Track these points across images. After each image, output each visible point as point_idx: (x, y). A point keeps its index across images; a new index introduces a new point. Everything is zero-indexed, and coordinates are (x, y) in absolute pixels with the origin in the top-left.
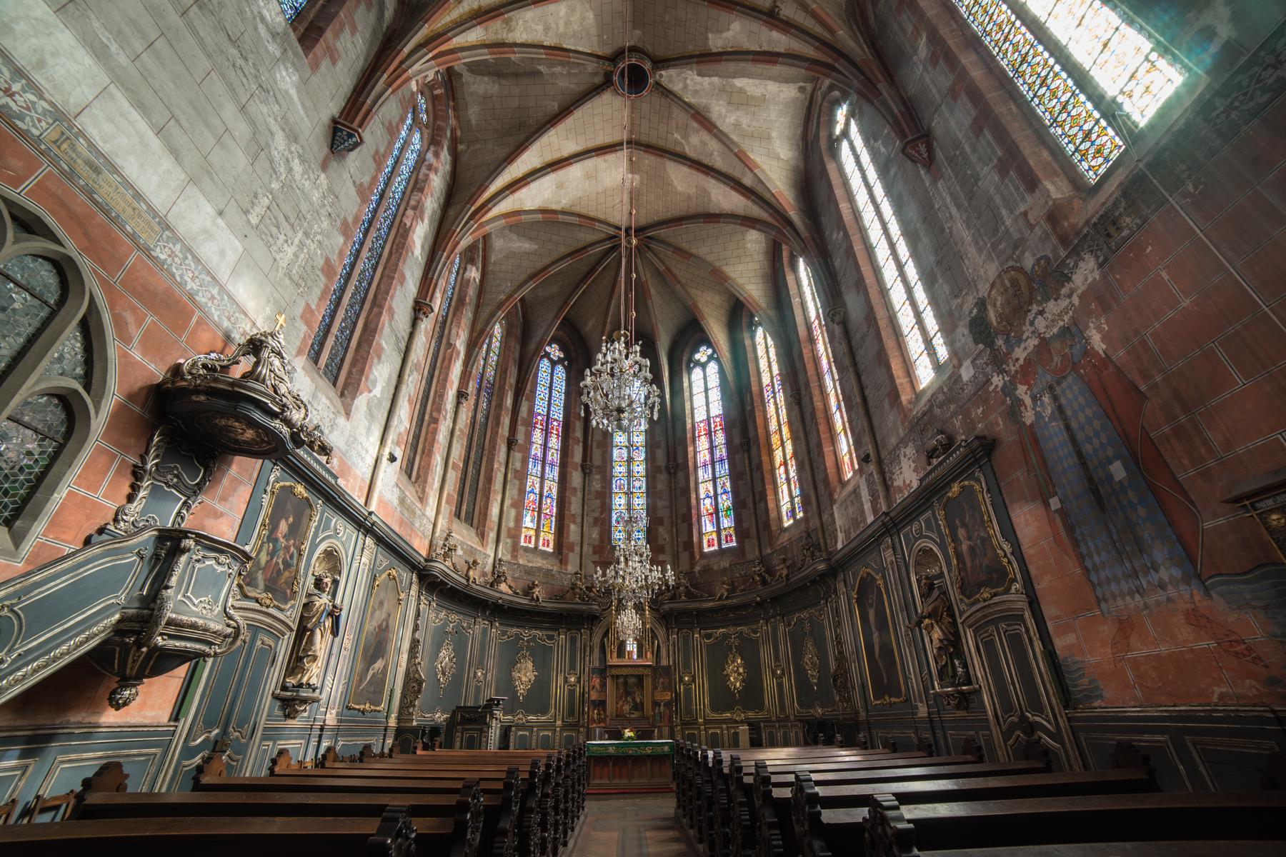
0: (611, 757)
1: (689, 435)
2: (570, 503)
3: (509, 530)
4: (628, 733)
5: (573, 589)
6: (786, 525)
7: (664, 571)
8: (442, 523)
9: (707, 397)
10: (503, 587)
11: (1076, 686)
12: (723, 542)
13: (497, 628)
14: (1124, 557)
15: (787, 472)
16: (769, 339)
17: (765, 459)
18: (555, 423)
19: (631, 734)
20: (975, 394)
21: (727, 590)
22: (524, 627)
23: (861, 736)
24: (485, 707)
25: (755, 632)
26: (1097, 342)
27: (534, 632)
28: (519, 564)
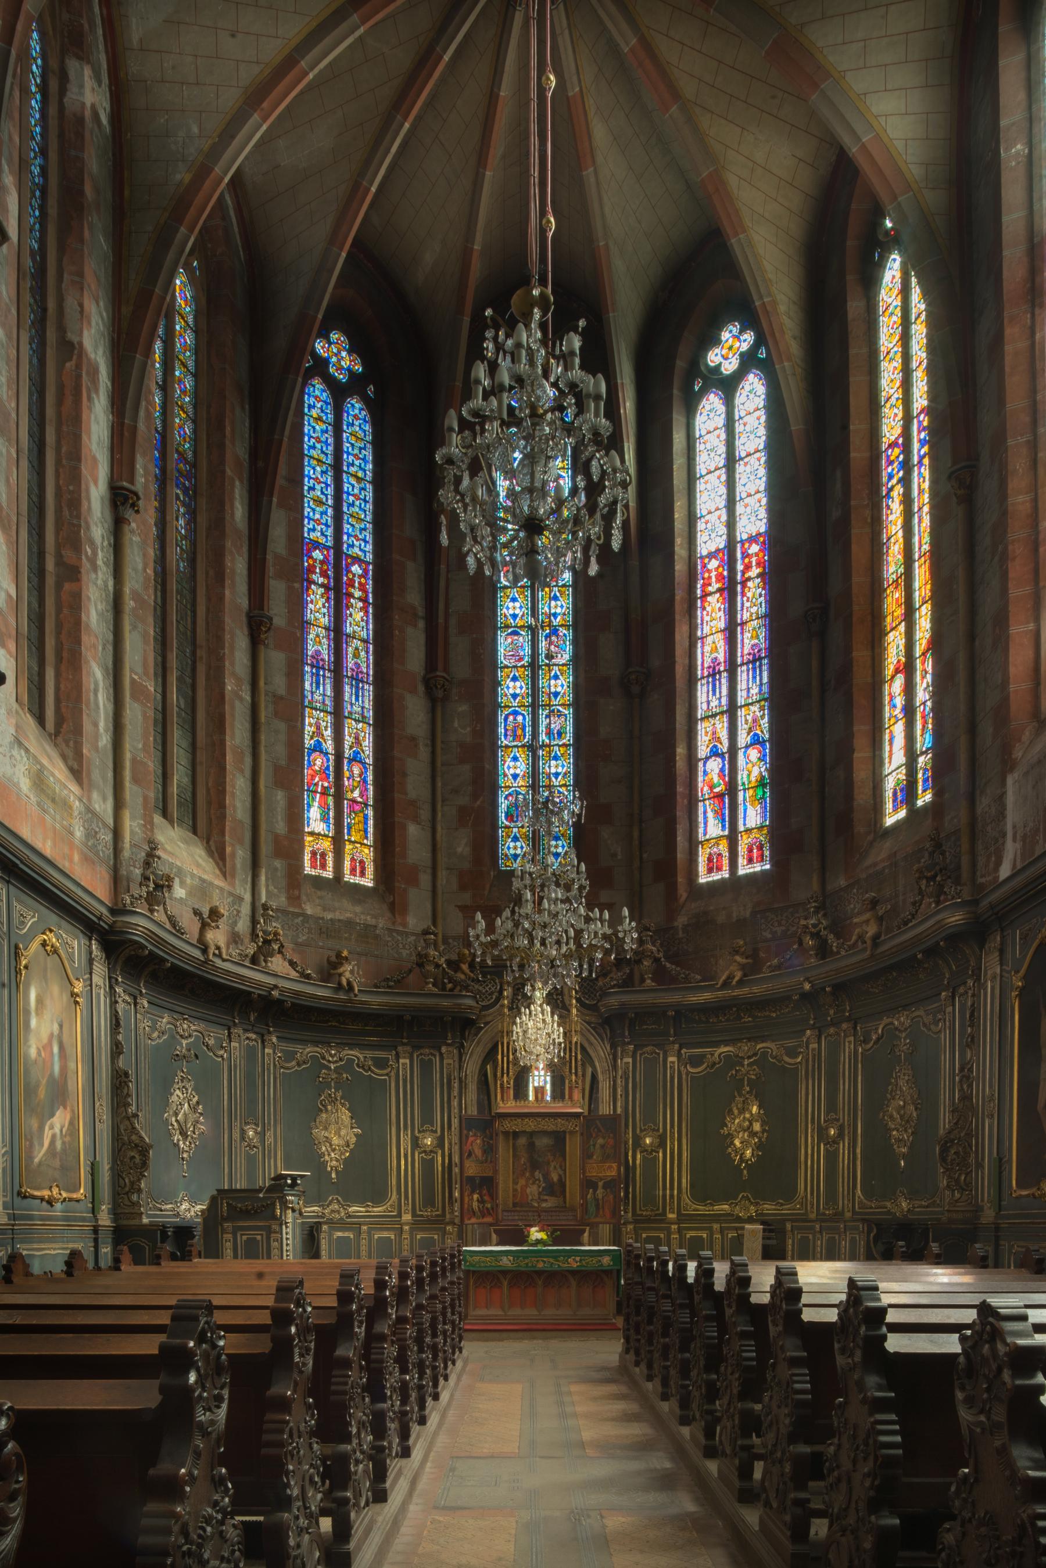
1: (680, 595)
2: (404, 775)
3: (277, 839)
4: (536, 1234)
6: (889, 821)
7: (616, 920)
8: (131, 825)
9: (731, 484)
10: (277, 964)
12: (742, 861)
13: (274, 1047)
15: (909, 689)
16: (916, 294)
17: (860, 654)
18: (356, 569)
19: (542, 1235)
22: (327, 1044)
23: (979, 1248)
24: (270, 1189)
28: (304, 915)
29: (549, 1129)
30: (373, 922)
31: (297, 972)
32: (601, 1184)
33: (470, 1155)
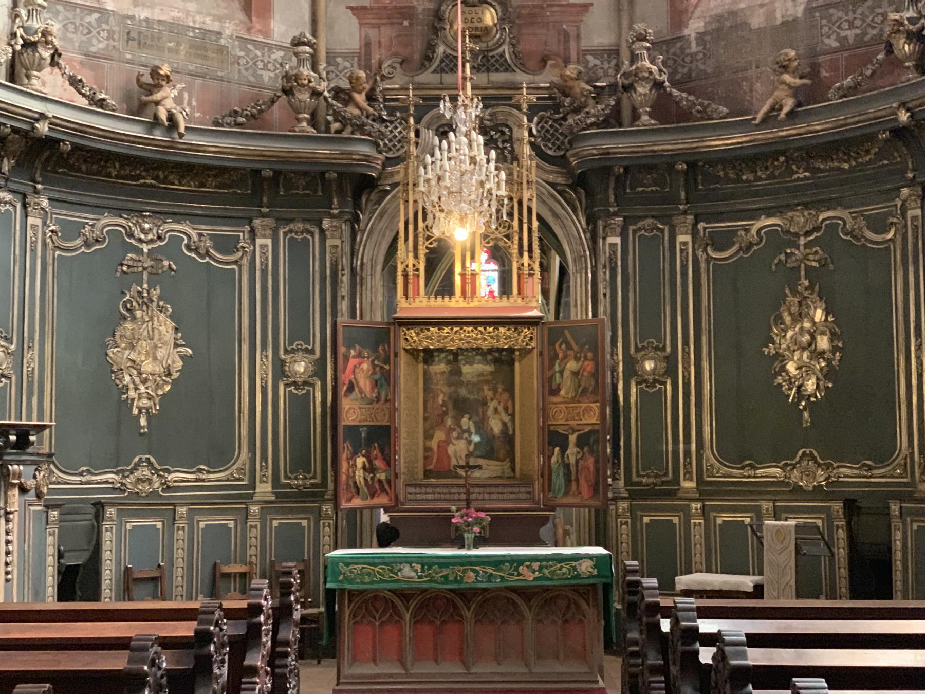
0: (405, 595)
5: (287, 92)
21: (795, 91)
25: (878, 226)
27: (171, 227)
29: (485, 345)
30: (216, 26)
31: (84, 95)
32: (573, 438)
33: (351, 388)
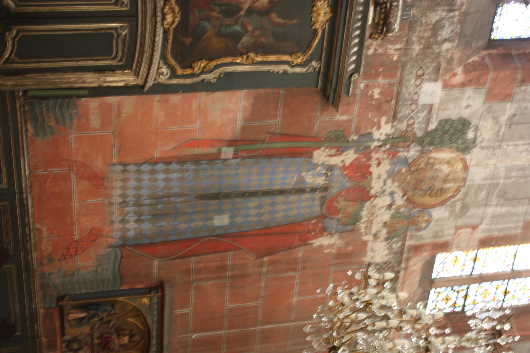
11: (48, 110)
14: (154, 201)
20: (398, 93)
26: (324, 241)
